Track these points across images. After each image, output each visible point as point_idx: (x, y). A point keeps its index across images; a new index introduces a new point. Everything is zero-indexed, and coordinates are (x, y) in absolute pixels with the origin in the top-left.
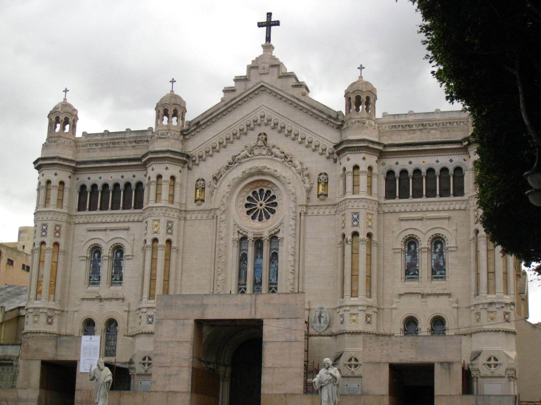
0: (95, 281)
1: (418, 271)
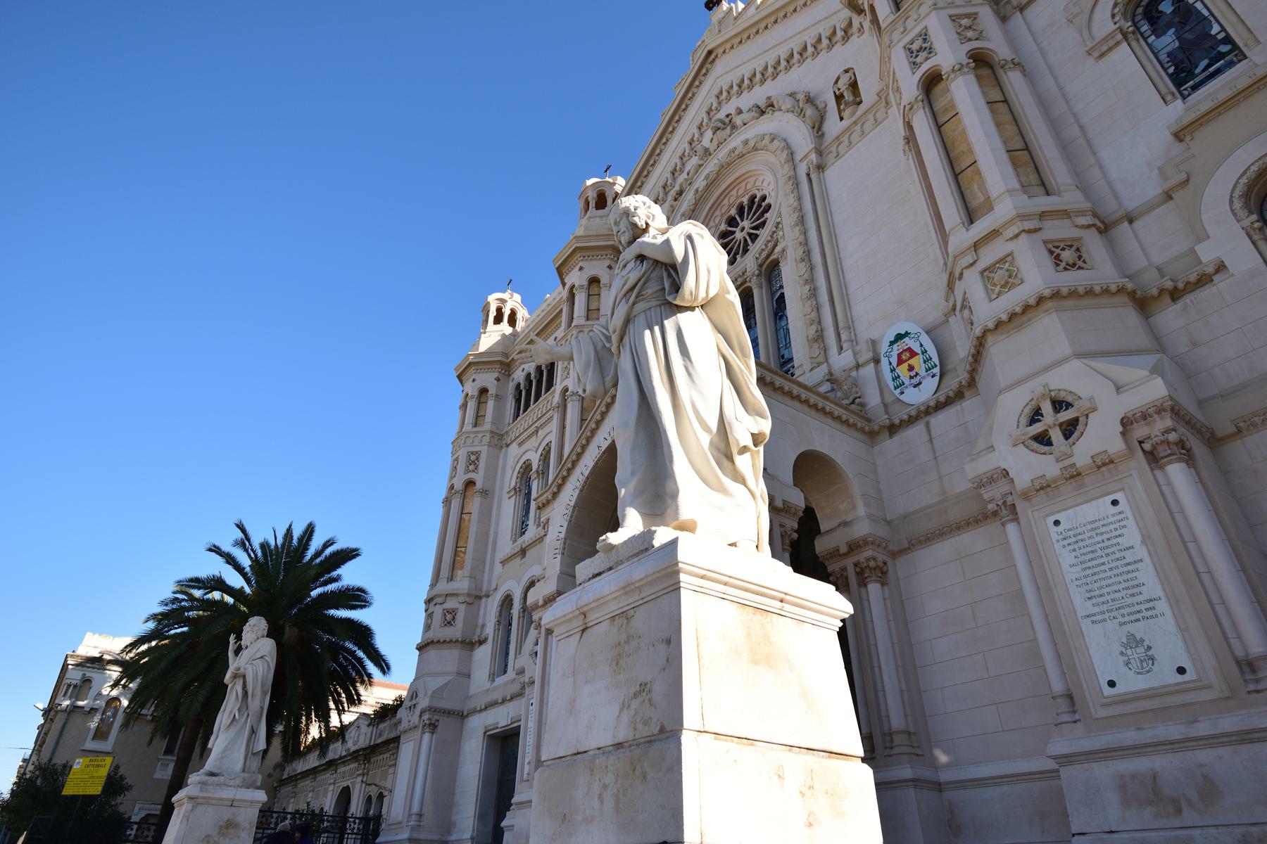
1: (1228, 40)
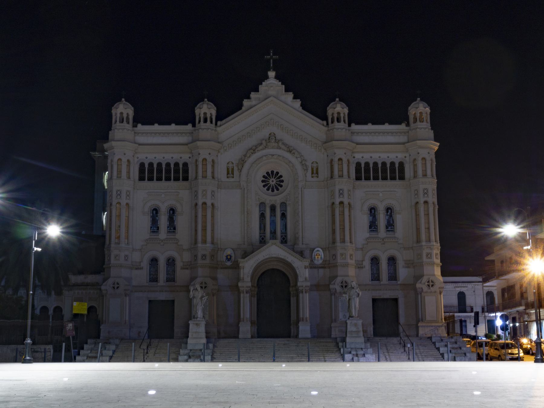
0: (155, 230)
1: (377, 226)
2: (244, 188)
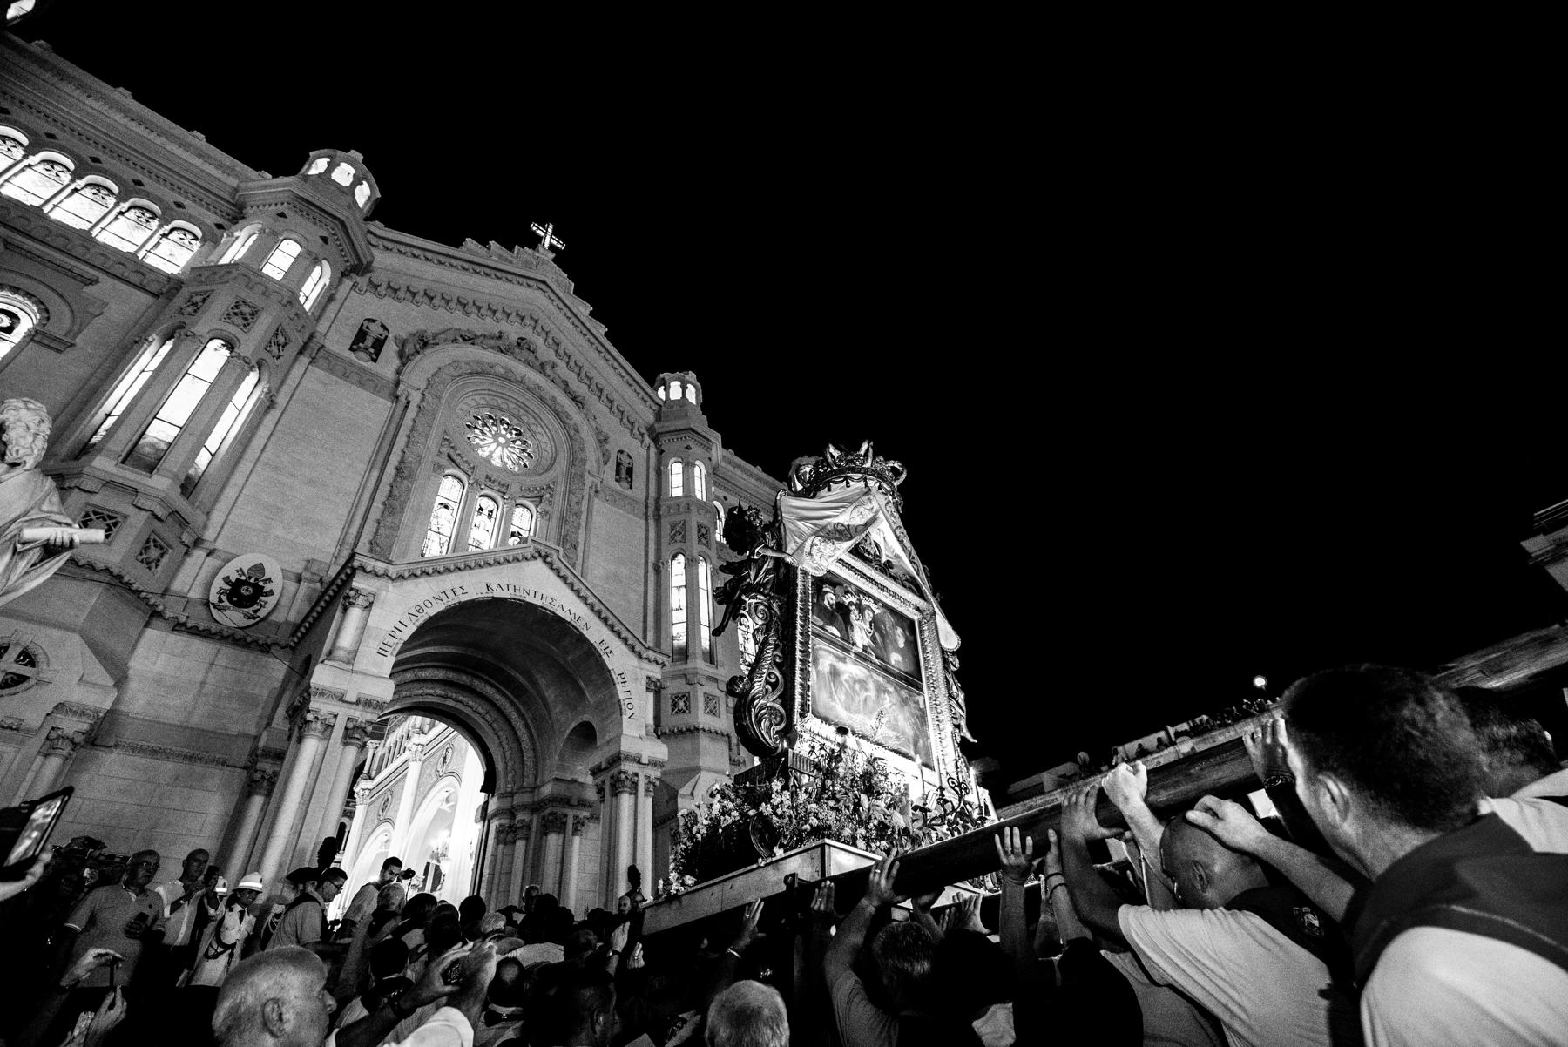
2: (408, 403)
